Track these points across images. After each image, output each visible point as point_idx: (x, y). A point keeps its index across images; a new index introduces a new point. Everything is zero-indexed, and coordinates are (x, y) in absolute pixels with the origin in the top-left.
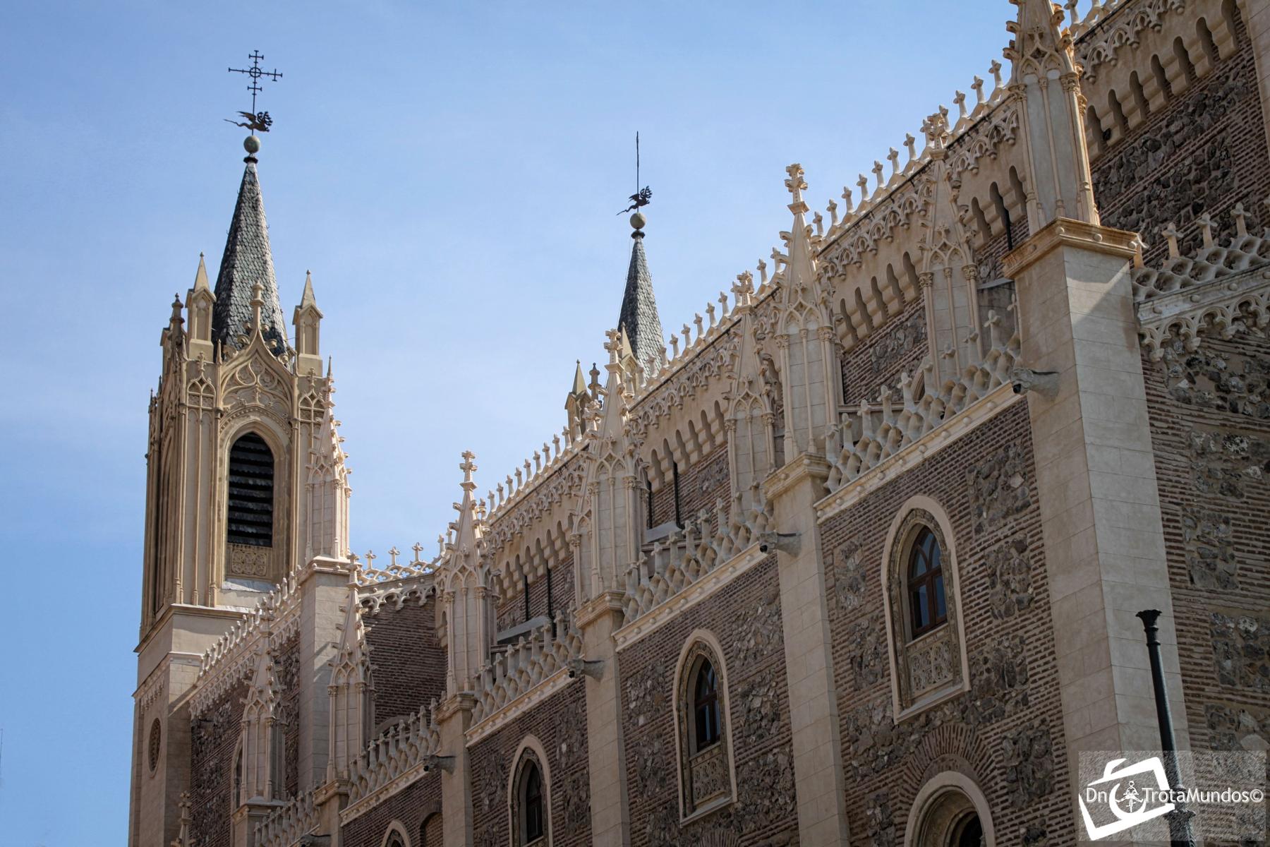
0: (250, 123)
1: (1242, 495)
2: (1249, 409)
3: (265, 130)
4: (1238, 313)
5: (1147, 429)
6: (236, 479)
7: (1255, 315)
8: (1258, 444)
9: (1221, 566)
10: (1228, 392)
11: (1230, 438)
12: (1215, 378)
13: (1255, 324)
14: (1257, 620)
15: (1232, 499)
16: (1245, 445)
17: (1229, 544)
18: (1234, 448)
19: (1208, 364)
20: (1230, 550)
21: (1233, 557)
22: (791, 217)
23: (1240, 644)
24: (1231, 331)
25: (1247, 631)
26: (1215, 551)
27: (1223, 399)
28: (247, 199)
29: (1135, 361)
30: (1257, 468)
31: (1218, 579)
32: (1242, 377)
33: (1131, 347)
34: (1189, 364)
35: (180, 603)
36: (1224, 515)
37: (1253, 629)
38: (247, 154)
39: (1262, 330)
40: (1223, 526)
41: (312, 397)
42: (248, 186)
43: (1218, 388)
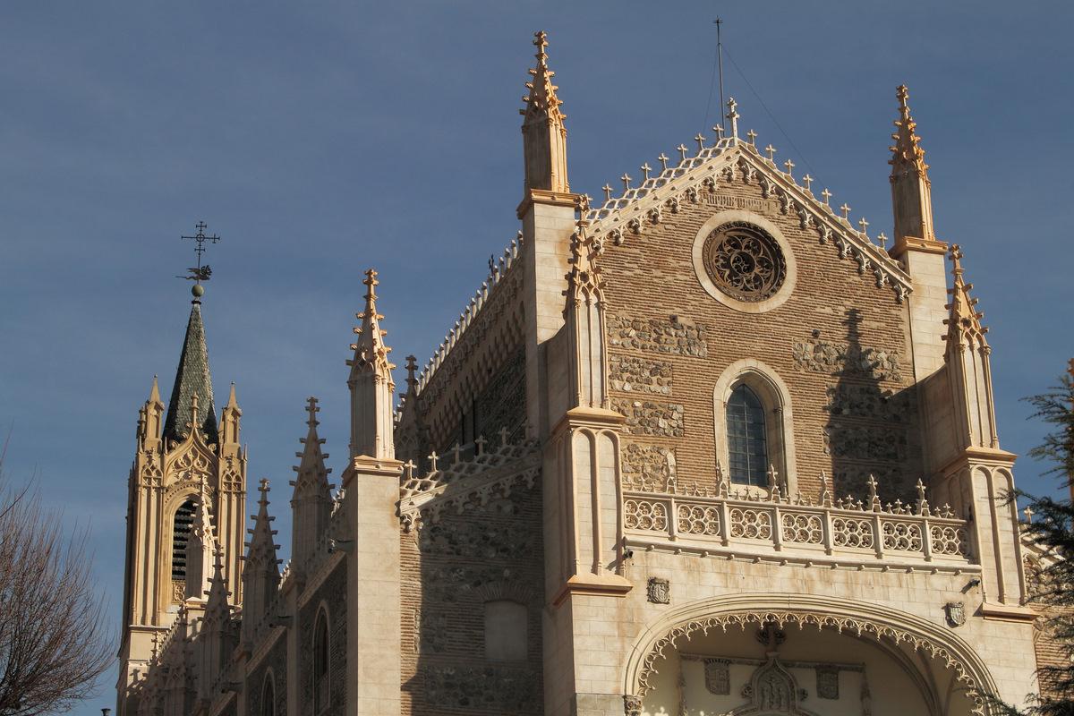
0: (195, 275)
1: (456, 601)
2: (468, 553)
3: (208, 279)
4: (468, 499)
5: (398, 570)
6: (178, 534)
7: (480, 499)
8: (471, 572)
9: (437, 640)
10: (456, 544)
11: (453, 570)
12: (449, 537)
13: (480, 505)
14: (455, 668)
15: (450, 604)
16: (462, 573)
17: (443, 628)
18: (455, 575)
19: (445, 529)
20: (444, 631)
21: (445, 634)
22: (307, 428)
23: (442, 681)
24: (460, 510)
25: (448, 675)
26: (434, 632)
27: (453, 548)
28: (192, 333)
29: (397, 532)
30: (468, 586)
31: (434, 647)
32: (467, 535)
33: (394, 526)
34: (433, 531)
35: (139, 624)
36: (442, 612)
37: (451, 673)
38: (193, 298)
40: (441, 619)
41: (233, 473)
42: (193, 322)
43: (450, 543)
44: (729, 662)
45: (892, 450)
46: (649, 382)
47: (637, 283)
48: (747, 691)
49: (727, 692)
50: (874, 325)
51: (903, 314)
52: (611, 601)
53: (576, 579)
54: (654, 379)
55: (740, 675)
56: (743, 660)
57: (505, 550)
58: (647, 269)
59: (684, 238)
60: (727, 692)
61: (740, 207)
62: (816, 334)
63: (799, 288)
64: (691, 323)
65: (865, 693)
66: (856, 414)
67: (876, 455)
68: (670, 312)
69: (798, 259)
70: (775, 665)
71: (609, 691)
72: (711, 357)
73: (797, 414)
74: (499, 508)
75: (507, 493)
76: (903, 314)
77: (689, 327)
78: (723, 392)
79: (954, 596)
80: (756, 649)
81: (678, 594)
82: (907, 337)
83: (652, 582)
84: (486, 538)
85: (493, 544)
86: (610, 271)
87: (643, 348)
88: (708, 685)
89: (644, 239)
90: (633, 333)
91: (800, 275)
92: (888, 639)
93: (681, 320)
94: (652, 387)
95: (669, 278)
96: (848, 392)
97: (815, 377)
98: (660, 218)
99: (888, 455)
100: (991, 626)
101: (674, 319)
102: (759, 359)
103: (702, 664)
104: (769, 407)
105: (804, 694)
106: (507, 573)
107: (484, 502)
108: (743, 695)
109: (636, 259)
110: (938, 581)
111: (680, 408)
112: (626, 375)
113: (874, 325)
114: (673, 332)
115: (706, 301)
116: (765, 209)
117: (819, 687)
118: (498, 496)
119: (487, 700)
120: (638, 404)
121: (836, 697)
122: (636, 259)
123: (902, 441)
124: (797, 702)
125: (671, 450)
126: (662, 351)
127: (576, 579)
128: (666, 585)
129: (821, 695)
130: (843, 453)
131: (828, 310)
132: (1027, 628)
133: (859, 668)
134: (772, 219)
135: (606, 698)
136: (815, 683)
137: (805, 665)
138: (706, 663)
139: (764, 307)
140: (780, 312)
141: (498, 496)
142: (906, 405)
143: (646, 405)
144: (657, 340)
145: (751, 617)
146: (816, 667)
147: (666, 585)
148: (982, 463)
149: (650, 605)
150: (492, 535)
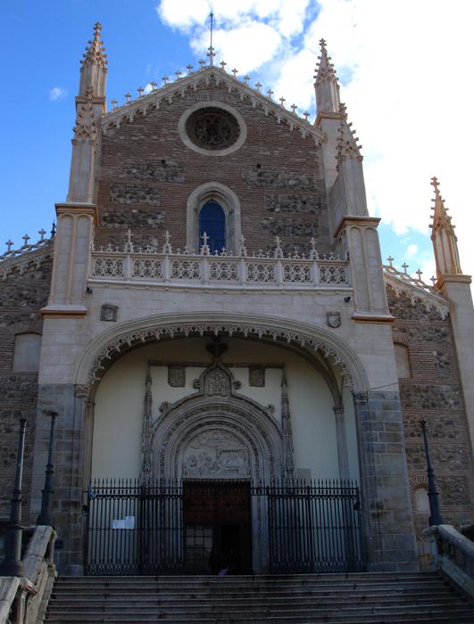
39: (22, 275)
44: (185, 365)
45: (308, 231)
46: (144, 198)
47: (140, 143)
48: (196, 385)
49: (183, 385)
50: (298, 160)
51: (317, 154)
52: (72, 321)
53: (50, 307)
54: (148, 196)
55: (192, 374)
56: (194, 365)
57: (32, 302)
58: (148, 136)
59: (174, 118)
60: (183, 385)
61: (211, 100)
62: (259, 166)
63: (248, 141)
64: (174, 164)
65: (284, 382)
66: (284, 211)
67: (297, 234)
68: (161, 158)
69: (248, 126)
70: (218, 366)
71: (65, 380)
72: (186, 182)
73: (242, 214)
74: (33, 276)
75: (38, 266)
76: (317, 154)
77: (174, 166)
78: (191, 203)
79: (329, 309)
80: (207, 358)
81: (124, 316)
82: (321, 168)
83: (105, 307)
84: (21, 295)
85: (26, 299)
86: (122, 138)
87: (142, 180)
88: (169, 382)
89: (147, 119)
90: (135, 171)
91: (248, 136)
92: (282, 338)
93: (167, 162)
94: (146, 201)
95: (162, 140)
96: (279, 199)
97: (257, 191)
98: (158, 107)
99: (306, 235)
100: (360, 327)
101: (163, 161)
102: (219, 182)
103: (166, 369)
104: (227, 213)
105: (238, 385)
106: (33, 315)
107: (21, 273)
108: (195, 387)
109: (141, 130)
110: (320, 300)
111: (163, 212)
112: (128, 195)
113: (298, 160)
114: (162, 169)
115: (185, 151)
116: (228, 99)
117: (250, 379)
118: (32, 269)
119: (9, 397)
120: (134, 211)
121: (263, 385)
122: (141, 130)
123: (316, 226)
124: (233, 390)
125: (156, 237)
126: (155, 180)
127: (50, 307)
128: (114, 309)
129: (252, 384)
130: (274, 234)
131: (268, 153)
132: (387, 327)
133: (281, 366)
134: (233, 105)
135: (61, 387)
136: (248, 378)
137: (240, 365)
138: (170, 366)
139: (224, 153)
140: (237, 154)
141: (32, 269)
142: (319, 204)
143: (140, 212)
144: (151, 174)
145: (194, 328)
146: (249, 367)
147: (114, 309)
148: (354, 224)
149: (102, 323)
150: (25, 293)
